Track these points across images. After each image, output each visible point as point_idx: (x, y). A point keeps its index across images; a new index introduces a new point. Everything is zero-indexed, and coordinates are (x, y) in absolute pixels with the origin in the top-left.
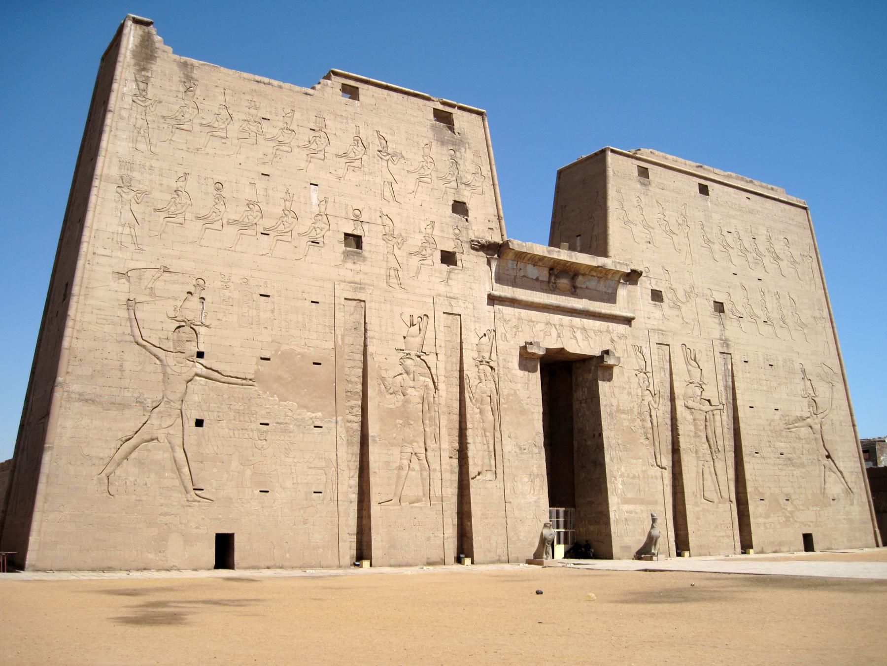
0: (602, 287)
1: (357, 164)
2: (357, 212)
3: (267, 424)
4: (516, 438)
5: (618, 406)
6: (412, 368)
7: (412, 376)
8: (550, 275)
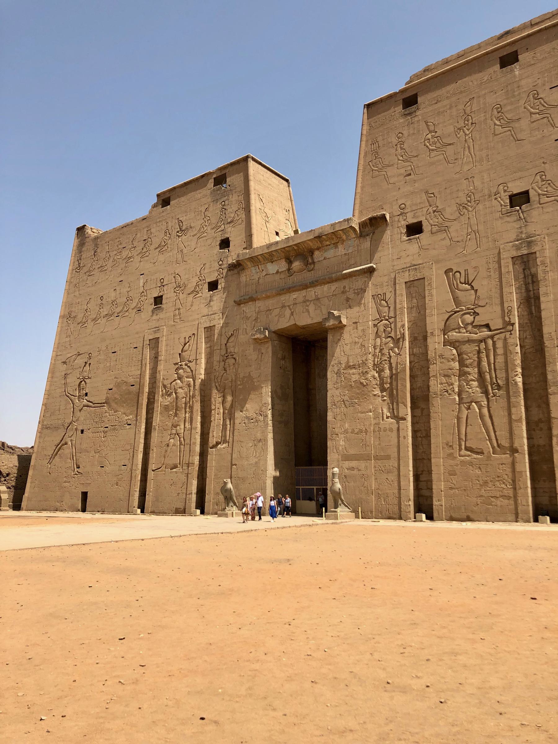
0: (341, 250)
1: (166, 247)
5: (348, 362)
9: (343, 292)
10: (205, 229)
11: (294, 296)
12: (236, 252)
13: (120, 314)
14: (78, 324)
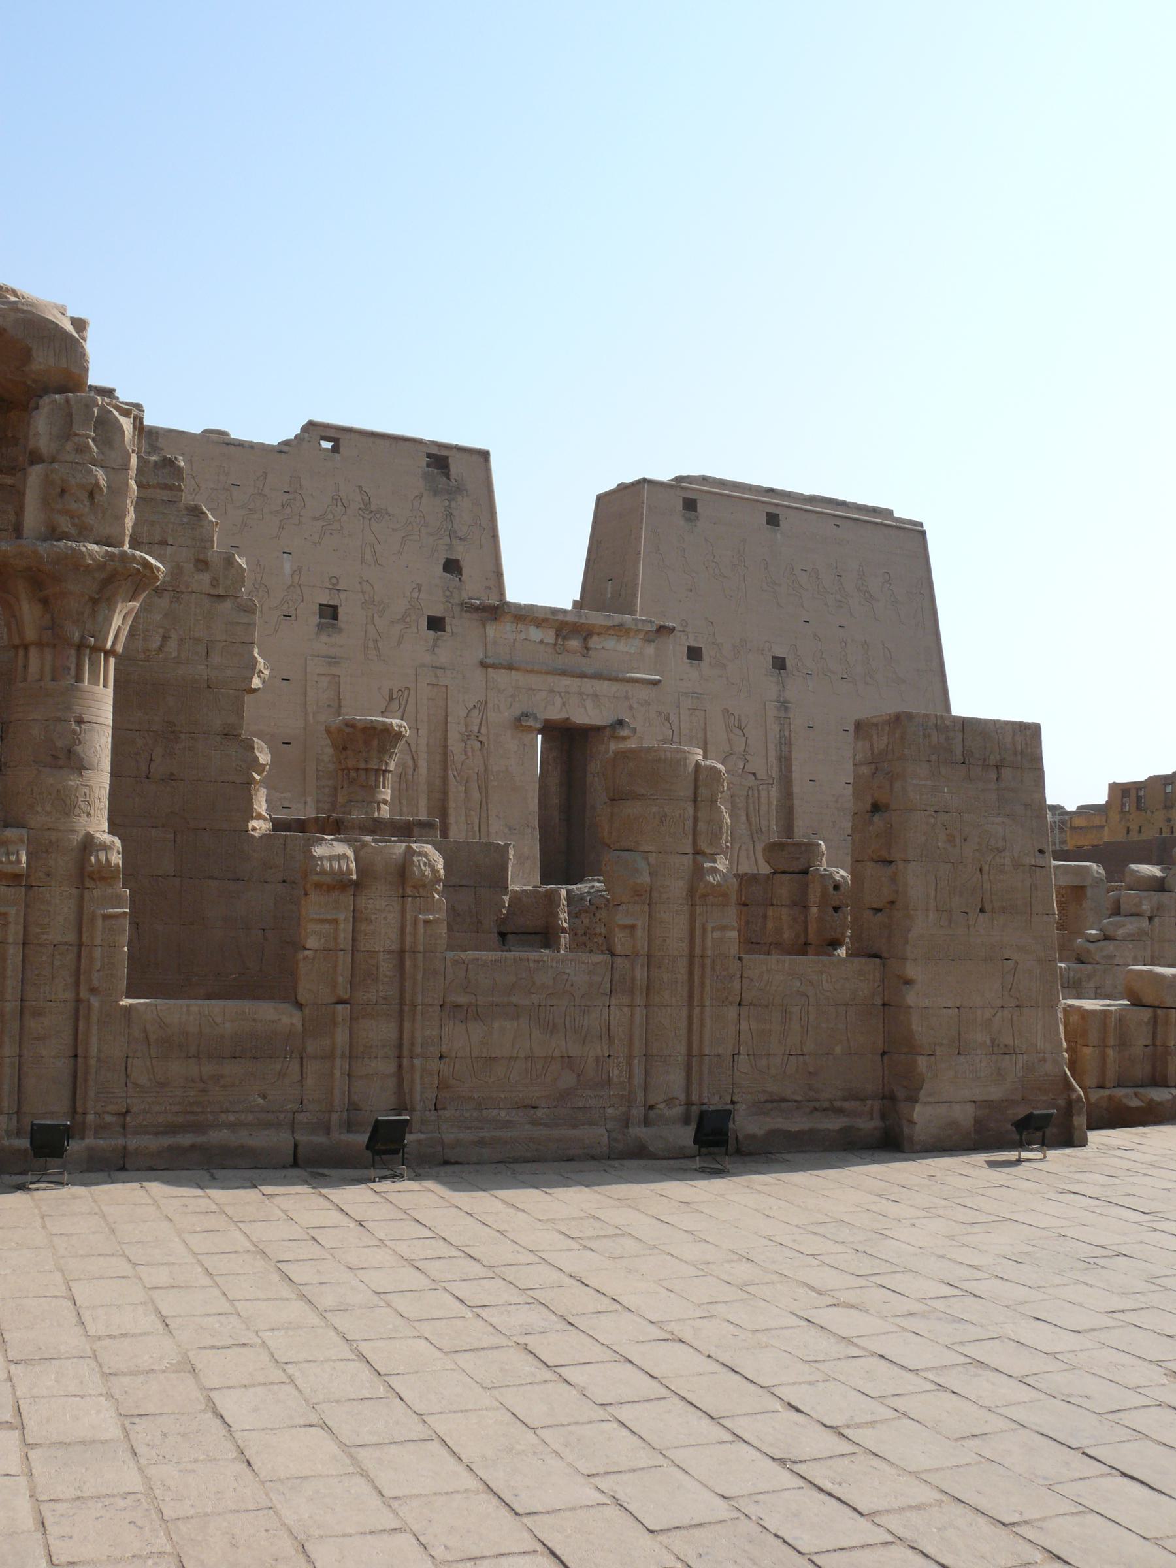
2: (334, 581)
8: (557, 636)
11: (568, 683)
12: (472, 587)
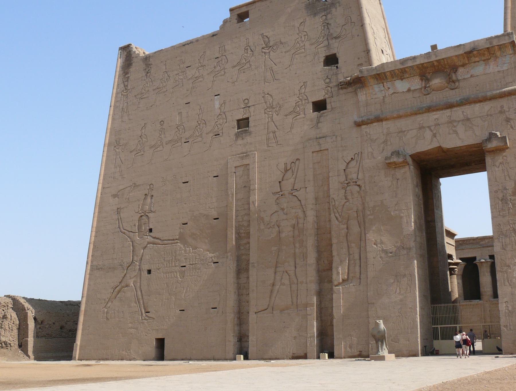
0: (492, 68)
1: (248, 65)
3: (185, 266)
4: (382, 243)
6: (285, 205)
7: (285, 211)
8: (422, 80)
9: (501, 112)
10: (302, 45)
11: (436, 117)
13: (190, 140)
14: (131, 152)
